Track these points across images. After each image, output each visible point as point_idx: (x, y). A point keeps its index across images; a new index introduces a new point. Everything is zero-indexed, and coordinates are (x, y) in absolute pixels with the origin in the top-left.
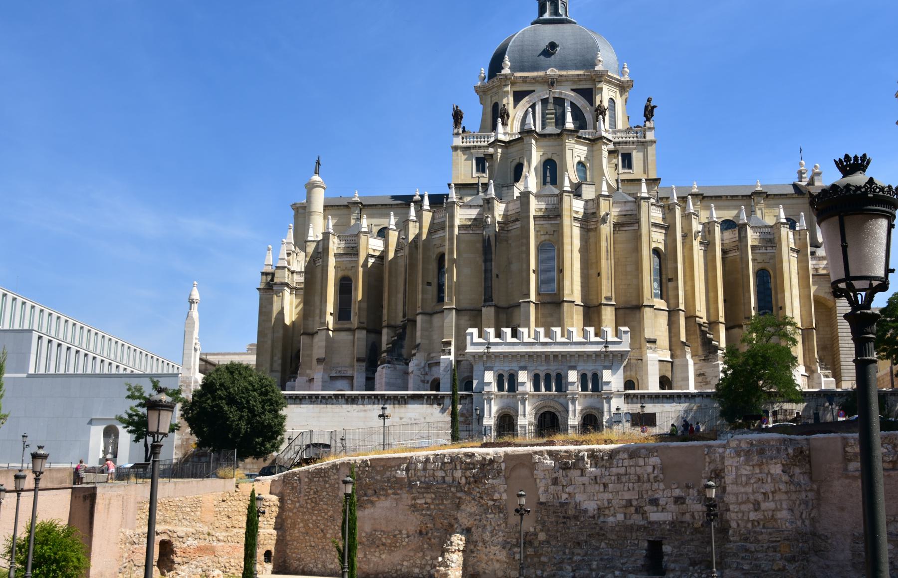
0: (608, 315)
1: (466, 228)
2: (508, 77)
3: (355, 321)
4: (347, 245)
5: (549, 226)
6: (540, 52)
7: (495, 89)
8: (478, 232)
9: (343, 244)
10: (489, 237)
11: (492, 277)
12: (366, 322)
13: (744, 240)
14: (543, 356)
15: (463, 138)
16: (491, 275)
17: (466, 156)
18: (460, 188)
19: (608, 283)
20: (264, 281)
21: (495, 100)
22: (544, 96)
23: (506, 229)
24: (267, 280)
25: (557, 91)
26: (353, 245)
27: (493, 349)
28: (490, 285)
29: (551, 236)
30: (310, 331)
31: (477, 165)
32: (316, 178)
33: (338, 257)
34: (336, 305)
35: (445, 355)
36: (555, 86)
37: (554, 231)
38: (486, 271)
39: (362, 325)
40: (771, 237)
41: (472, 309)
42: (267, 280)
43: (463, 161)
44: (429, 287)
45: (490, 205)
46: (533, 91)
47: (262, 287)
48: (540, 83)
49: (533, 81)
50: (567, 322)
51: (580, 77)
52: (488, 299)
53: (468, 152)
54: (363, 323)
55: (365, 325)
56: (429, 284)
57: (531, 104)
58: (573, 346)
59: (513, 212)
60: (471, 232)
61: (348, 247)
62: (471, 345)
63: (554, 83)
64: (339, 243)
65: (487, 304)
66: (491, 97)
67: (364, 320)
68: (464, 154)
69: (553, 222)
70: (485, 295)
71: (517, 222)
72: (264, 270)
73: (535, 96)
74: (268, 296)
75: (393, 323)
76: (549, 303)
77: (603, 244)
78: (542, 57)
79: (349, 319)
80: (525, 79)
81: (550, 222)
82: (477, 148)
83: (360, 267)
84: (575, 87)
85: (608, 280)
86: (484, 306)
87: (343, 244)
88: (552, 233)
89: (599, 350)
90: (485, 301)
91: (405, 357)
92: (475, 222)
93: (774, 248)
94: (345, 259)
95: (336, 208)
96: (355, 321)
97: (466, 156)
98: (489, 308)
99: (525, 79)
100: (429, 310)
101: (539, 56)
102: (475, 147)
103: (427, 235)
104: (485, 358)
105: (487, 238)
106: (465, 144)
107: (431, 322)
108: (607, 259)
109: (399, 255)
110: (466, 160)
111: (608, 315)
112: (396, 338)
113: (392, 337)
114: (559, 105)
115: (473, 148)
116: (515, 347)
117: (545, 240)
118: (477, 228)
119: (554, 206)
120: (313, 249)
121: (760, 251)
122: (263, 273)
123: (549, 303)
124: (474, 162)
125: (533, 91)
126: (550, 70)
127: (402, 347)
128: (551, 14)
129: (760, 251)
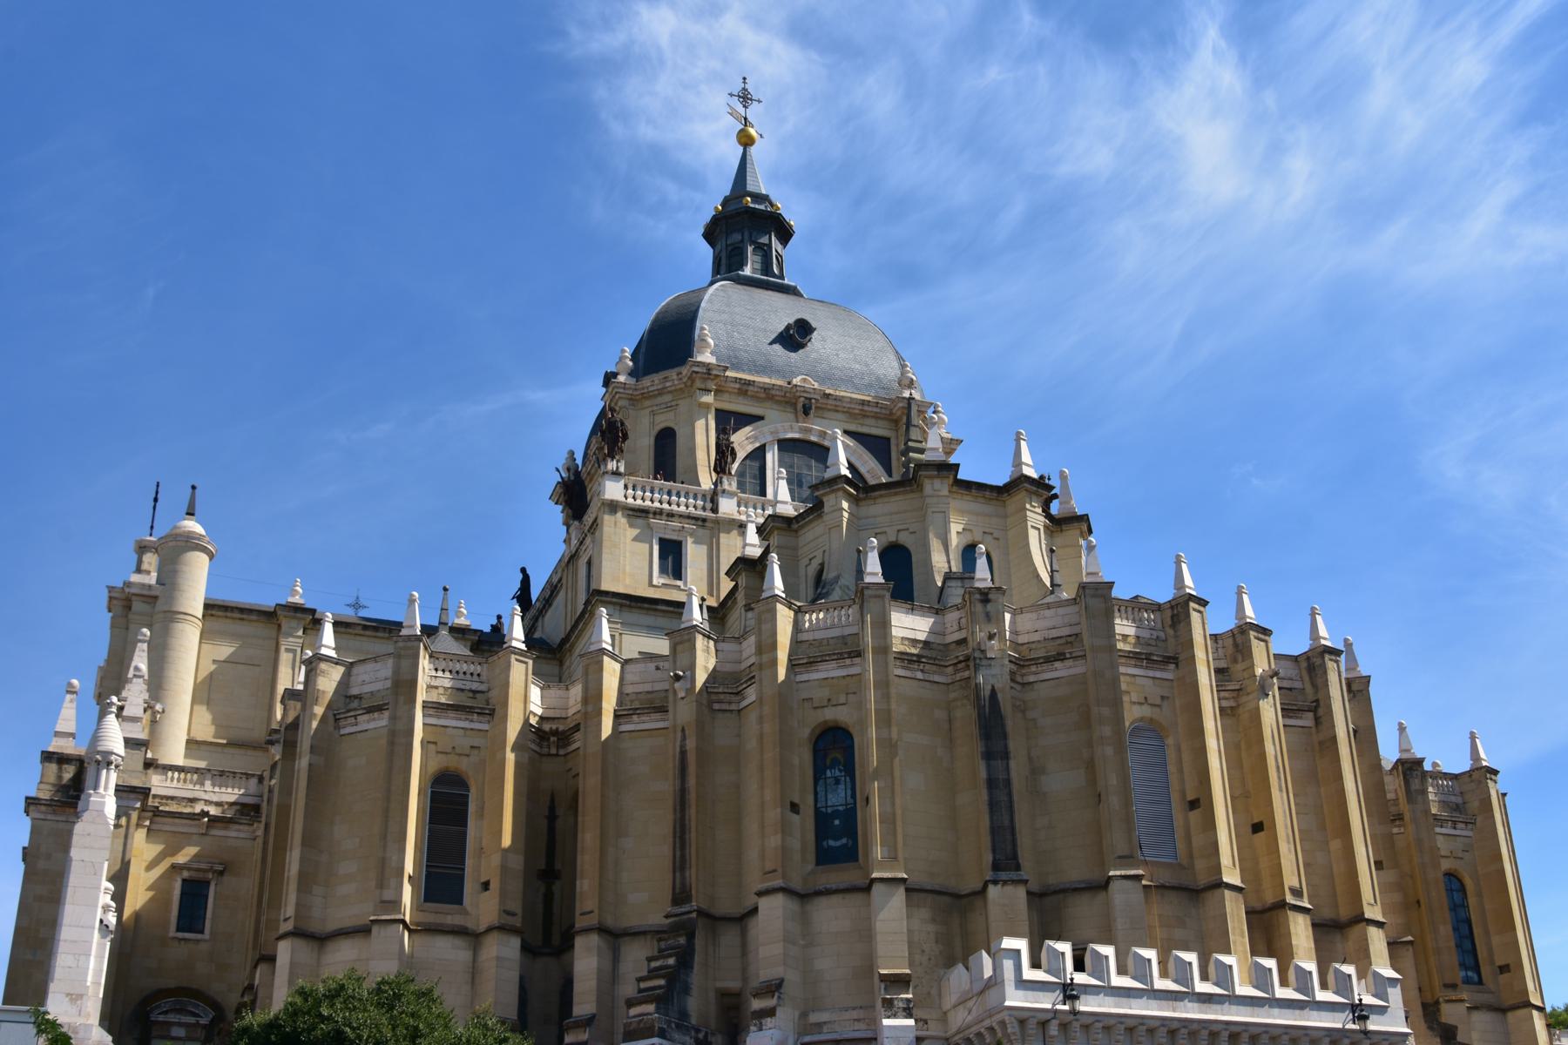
0: (1300, 932)
1: (910, 661)
2: (714, 372)
3: (482, 908)
4: (460, 685)
5: (1150, 682)
6: (773, 336)
7: (667, 398)
8: (937, 678)
9: (446, 681)
10: (993, 690)
11: (1011, 802)
12: (519, 911)
13: (1420, 797)
14: (1205, 1033)
15: (626, 487)
16: (1010, 795)
17: (636, 532)
18: (622, 605)
19: (1290, 851)
20: (52, 778)
21: (663, 421)
22: (785, 432)
23: (1019, 679)
24: (60, 777)
25: (815, 429)
26: (475, 686)
27: (1087, 1005)
28: (1007, 823)
29: (1157, 710)
30: (315, 927)
31: (662, 557)
32: (193, 526)
33: (431, 712)
34: (422, 853)
35: (895, 1016)
36: (812, 415)
37: (1163, 698)
38: (991, 783)
39: (510, 921)
40: (1459, 800)
41: (937, 888)
42: (60, 777)
43: (628, 540)
44: (795, 818)
45: (989, 607)
46: (761, 418)
47: (45, 795)
48: (778, 402)
49: (763, 395)
50: (1235, 942)
51: (866, 408)
52: (1005, 862)
53: (640, 521)
54: (514, 914)
55: (517, 922)
56: (794, 808)
57: (757, 445)
58: (1276, 1011)
59: (1036, 637)
60: (919, 675)
61: (462, 690)
62: (1017, 988)
63: (810, 408)
64: (434, 673)
65: (1004, 875)
66: (653, 413)
67: (516, 906)
68: (631, 526)
69: (1158, 674)
70: (994, 851)
71: (1057, 664)
72: (57, 745)
73: (766, 429)
74: (61, 826)
75: (610, 922)
76: (1173, 888)
77: (1270, 749)
78: (777, 347)
79: (458, 899)
80: (745, 387)
81: (1151, 673)
82: (664, 517)
83: (508, 749)
84: (852, 428)
85: (1289, 842)
86: (995, 882)
87: (446, 681)
88: (1158, 701)
89: (1339, 1026)
90: (996, 867)
91: (694, 1021)
92: (926, 653)
93: (1470, 826)
94: (450, 721)
95: (238, 615)
96: (482, 908)
97: (636, 532)
98: (1009, 889)
99: (745, 387)
100: (796, 884)
101: (771, 344)
102: (658, 513)
103: (788, 669)
104: (1053, 1029)
105: (987, 693)
106: (639, 502)
107: (805, 920)
108: (1281, 790)
109: (623, 728)
110: (636, 539)
111: (1300, 932)
112: (671, 961)
113: (650, 960)
114: (816, 460)
115: (655, 513)
116: (1134, 1002)
117: (1141, 719)
118: (934, 668)
119: (1154, 633)
120: (334, 685)
121: (1444, 831)
122: (48, 757)
123: (1173, 888)
124: (656, 548)
125: (761, 418)
126: (799, 378)
127: (686, 990)
128: (754, 270)
129: (1444, 831)
